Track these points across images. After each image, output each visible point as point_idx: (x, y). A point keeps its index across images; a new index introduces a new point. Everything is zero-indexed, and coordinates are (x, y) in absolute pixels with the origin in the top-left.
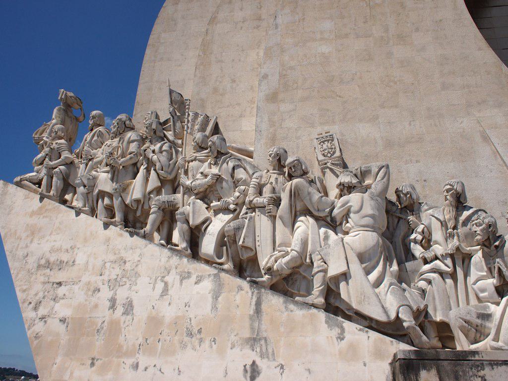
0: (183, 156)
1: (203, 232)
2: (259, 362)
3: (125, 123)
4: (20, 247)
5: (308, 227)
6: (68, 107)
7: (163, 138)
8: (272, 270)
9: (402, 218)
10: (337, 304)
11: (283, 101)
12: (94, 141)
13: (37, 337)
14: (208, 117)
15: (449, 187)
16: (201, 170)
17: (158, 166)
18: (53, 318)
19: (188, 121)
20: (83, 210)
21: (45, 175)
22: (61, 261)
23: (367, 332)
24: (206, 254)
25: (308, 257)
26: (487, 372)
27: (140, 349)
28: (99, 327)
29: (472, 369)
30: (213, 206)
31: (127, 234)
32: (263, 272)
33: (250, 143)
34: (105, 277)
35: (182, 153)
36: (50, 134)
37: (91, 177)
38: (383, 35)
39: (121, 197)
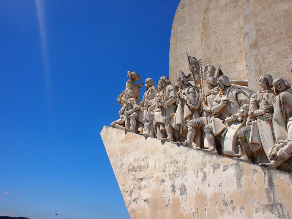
1: (223, 137)
3: (165, 81)
4: (118, 161)
6: (133, 80)
7: (189, 85)
8: (276, 156)
13: (133, 211)
14: (214, 67)
16: (215, 100)
17: (188, 101)
19: (202, 72)
20: (148, 135)
22: (140, 166)
24: (227, 152)
27: (194, 216)
28: (167, 203)
30: (227, 120)
31: (176, 145)
32: (269, 159)
33: (244, 78)
34: (167, 173)
35: (201, 92)
36: (126, 97)
37: (150, 115)
39: (169, 124)
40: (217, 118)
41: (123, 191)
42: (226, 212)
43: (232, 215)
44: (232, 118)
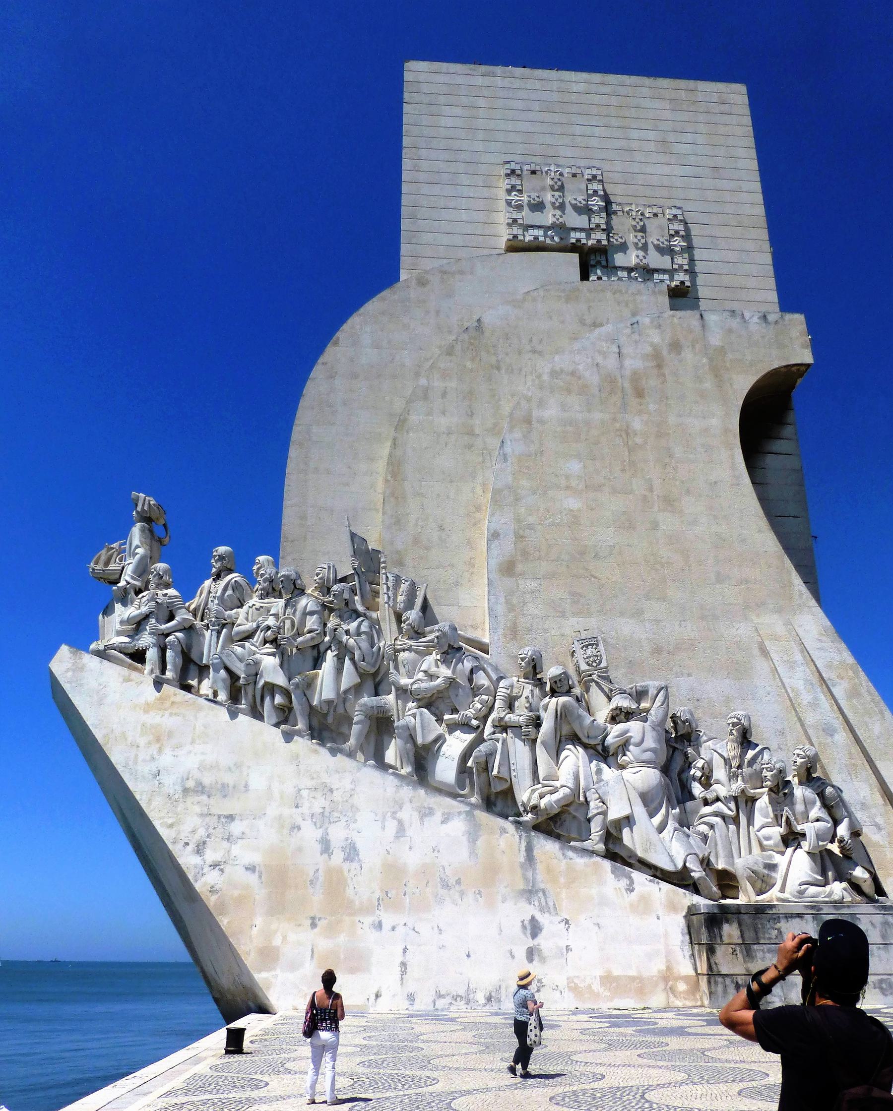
0: (389, 643)
2: (539, 917)
3: (294, 583)
4: (140, 759)
5: (578, 758)
8: (538, 809)
11: (522, 574)
12: (227, 596)
13: (213, 890)
15: (735, 720)
21: (154, 645)
23: (658, 883)
25: (581, 795)
27: (379, 904)
29: (769, 921)
34: (305, 809)
38: (647, 494)
40: (425, 710)
41: (172, 841)
43: (458, 905)
44: (459, 717)
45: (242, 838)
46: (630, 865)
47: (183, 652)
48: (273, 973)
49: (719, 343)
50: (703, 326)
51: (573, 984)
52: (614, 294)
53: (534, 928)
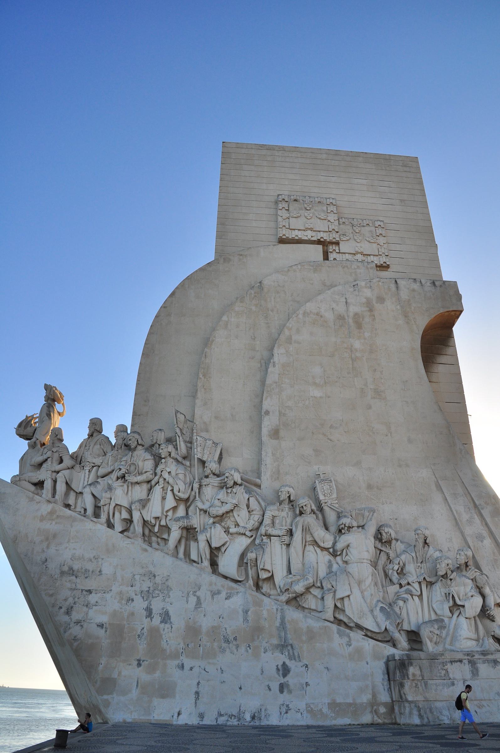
2: (288, 662)
3: (138, 441)
9: (383, 551)
10: (341, 617)
16: (217, 497)
18: (90, 623)
23: (367, 640)
26: (449, 666)
28: (139, 633)
42: (228, 650)
45: (96, 606)
46: (350, 628)
47: (67, 483)
48: (111, 696)
49: (407, 297)
50: (397, 288)
51: (310, 708)
52: (343, 268)
53: (285, 670)
